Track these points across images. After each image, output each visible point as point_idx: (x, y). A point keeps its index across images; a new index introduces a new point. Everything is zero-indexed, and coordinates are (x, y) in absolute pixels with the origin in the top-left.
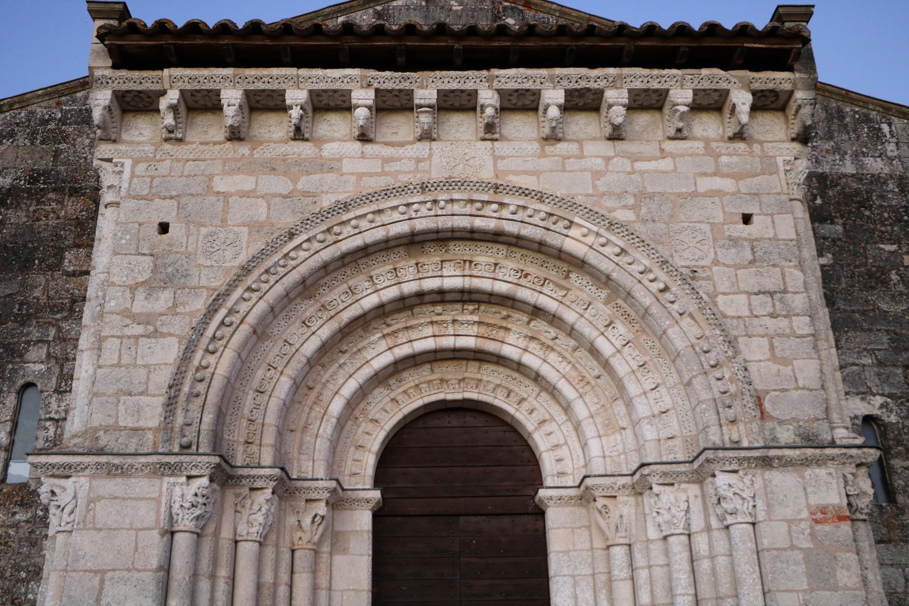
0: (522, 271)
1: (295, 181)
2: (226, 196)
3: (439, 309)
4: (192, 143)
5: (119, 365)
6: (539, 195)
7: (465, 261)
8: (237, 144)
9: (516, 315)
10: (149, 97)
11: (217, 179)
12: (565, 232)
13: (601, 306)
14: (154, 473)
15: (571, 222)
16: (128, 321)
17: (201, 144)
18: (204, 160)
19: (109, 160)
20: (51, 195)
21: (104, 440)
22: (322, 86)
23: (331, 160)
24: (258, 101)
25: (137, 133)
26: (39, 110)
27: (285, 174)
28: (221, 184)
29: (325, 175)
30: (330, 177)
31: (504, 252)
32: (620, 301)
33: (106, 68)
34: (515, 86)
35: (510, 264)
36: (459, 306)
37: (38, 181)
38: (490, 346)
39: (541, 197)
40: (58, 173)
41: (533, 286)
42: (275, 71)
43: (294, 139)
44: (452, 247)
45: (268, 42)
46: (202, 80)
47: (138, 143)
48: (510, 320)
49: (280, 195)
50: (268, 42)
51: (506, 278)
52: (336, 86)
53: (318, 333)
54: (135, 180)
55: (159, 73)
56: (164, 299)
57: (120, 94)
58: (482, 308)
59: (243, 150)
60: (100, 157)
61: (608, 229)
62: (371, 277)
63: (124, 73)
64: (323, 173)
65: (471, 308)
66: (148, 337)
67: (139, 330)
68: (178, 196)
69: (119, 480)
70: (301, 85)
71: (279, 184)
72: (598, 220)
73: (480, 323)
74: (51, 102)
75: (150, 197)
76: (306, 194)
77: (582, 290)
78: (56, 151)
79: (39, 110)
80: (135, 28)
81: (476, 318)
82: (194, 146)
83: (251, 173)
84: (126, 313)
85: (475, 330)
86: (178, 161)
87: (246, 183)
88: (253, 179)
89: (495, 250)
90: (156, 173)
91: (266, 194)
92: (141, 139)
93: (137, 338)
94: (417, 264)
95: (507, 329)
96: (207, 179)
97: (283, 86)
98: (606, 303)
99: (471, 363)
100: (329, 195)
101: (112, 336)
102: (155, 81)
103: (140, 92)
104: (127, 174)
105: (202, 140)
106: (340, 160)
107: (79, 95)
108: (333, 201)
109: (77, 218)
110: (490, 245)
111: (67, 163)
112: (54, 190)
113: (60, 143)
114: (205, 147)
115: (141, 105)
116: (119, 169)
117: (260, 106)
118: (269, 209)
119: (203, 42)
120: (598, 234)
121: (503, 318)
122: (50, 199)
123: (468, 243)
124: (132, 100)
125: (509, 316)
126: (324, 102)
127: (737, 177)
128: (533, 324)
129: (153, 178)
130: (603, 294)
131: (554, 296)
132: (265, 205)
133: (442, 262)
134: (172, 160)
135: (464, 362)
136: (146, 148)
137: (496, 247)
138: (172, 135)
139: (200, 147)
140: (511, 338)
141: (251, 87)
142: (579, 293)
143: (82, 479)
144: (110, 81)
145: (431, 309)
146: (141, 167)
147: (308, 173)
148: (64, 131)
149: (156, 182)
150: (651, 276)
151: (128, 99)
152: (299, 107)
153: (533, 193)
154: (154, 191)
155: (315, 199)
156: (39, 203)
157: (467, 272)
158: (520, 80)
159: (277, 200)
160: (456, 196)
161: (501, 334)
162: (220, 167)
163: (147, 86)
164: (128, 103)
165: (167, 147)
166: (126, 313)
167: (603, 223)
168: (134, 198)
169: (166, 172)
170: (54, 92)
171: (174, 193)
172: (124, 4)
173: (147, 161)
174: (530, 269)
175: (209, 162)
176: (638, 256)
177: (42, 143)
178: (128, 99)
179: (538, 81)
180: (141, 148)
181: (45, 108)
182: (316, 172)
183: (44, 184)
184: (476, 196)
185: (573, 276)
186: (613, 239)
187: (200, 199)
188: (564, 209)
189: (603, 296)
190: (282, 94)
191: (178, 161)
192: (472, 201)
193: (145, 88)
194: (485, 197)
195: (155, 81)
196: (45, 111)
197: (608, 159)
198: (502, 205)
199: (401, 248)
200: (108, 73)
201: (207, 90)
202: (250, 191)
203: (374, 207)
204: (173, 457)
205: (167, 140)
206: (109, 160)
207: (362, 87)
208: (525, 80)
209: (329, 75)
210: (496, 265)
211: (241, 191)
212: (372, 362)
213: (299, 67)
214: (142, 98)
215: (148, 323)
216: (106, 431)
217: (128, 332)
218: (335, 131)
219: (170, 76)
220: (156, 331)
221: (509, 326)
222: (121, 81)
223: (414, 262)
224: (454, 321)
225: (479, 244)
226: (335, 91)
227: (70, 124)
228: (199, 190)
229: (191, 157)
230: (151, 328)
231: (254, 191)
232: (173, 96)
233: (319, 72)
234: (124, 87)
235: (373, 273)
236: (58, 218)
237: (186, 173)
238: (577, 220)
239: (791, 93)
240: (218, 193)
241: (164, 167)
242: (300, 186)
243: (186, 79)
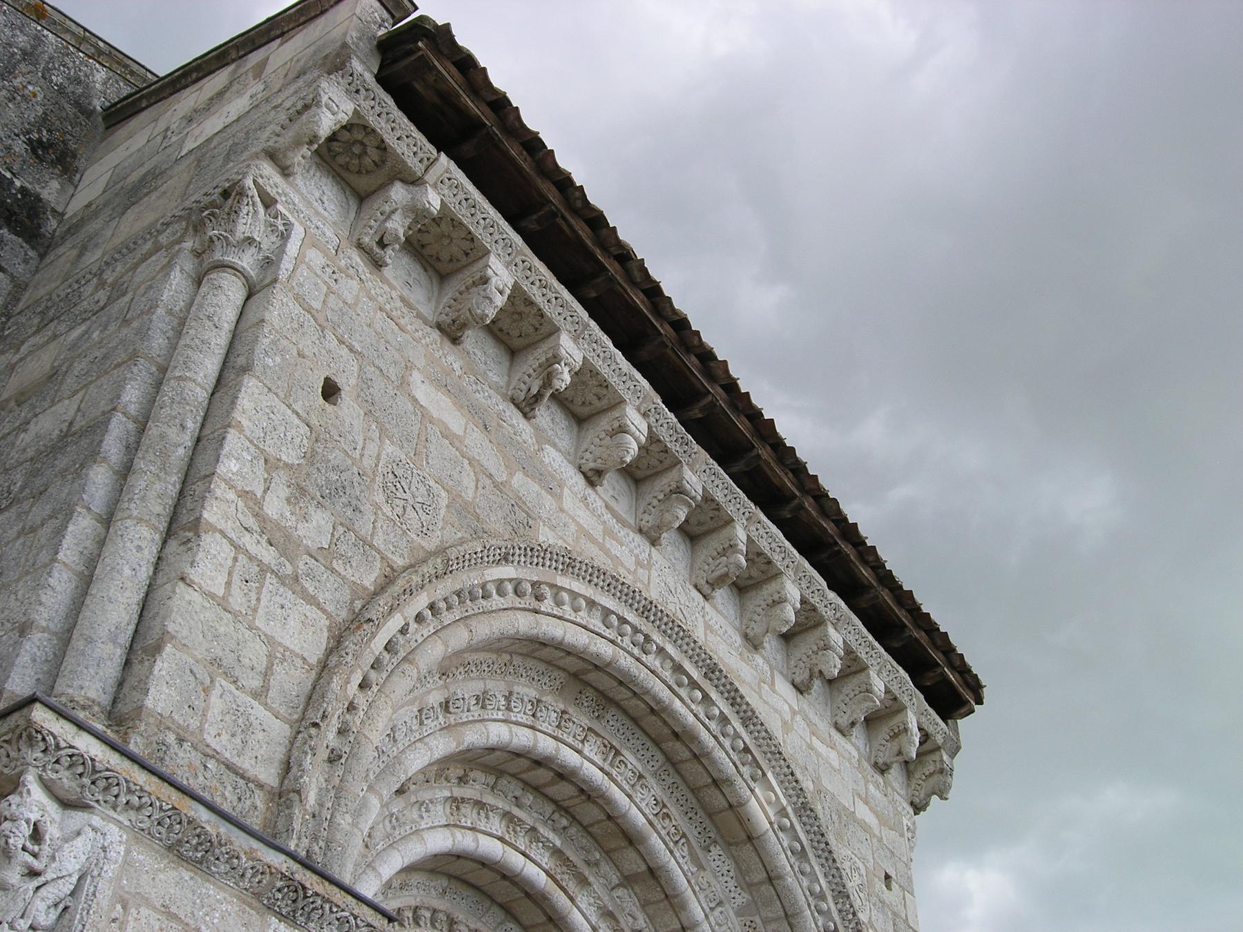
0: (664, 806)
3: (529, 799)
5: (223, 603)
6: (750, 714)
7: (612, 747)
9: (606, 867)
11: (415, 374)
12: (752, 784)
13: (731, 913)
14: (257, 896)
15: (764, 774)
16: (251, 522)
17: (403, 299)
21: (181, 762)
28: (423, 392)
31: (657, 765)
32: (757, 919)
34: (767, 551)
35: (657, 790)
36: (549, 808)
38: (560, 899)
39: (749, 718)
41: (667, 838)
44: (609, 716)
46: (479, 216)
48: (595, 869)
51: (643, 805)
52: (614, 380)
53: (427, 740)
56: (315, 528)
58: (573, 830)
61: (795, 810)
62: (511, 693)
65: (565, 822)
66: (282, 580)
67: (268, 555)
69: (187, 875)
72: (791, 792)
73: (557, 853)
77: (716, 877)
81: (558, 843)
84: (254, 503)
85: (546, 860)
89: (649, 754)
93: (264, 569)
94: (564, 712)
95: (583, 882)
98: (739, 913)
99: (495, 909)
101: (222, 532)
102: (421, 155)
110: (649, 744)
119: (531, 173)
120: (782, 812)
121: (588, 863)
123: (628, 723)
125: (597, 864)
127: (883, 821)
128: (620, 892)
130: (742, 898)
131: (686, 868)
133: (589, 729)
135: (487, 903)
137: (654, 750)
138: (377, 250)
140: (583, 900)
142: (713, 882)
143: (113, 829)
144: (363, 91)
145: (518, 793)
150: (824, 906)
153: (744, 707)
157: (607, 767)
158: (774, 545)
160: (670, 649)
161: (572, 886)
165: (357, 258)
166: (254, 503)
167: (795, 799)
171: (358, 347)
174: (673, 810)
176: (817, 868)
179: (787, 561)
184: (688, 666)
185: (716, 851)
186: (798, 827)
188: (765, 752)
189: (739, 900)
192: (678, 668)
193: (399, 151)
194: (695, 674)
195: (421, 155)
197: (794, 713)
198: (706, 696)
199: (563, 674)
203: (588, 591)
204: (315, 878)
207: (638, 410)
208: (778, 550)
210: (641, 777)
212: (426, 835)
215: (283, 554)
216: (181, 741)
217: (248, 541)
220: (296, 579)
221: (591, 879)
223: (562, 706)
224: (533, 829)
225: (639, 733)
228: (392, 372)
230: (289, 569)
234: (372, 120)
235: (516, 689)
238: (770, 775)
239: (938, 748)
243: (461, 196)
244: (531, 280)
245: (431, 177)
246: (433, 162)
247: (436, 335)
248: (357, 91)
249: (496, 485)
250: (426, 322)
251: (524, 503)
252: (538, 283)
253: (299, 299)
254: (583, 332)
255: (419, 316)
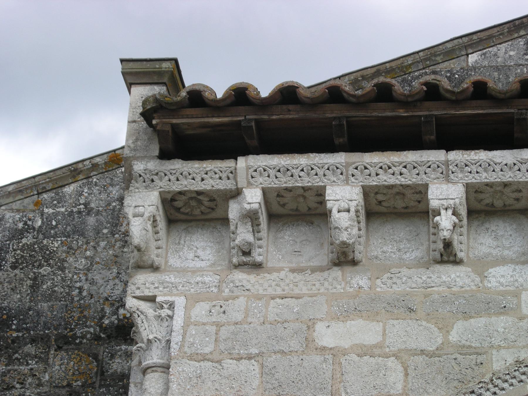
1: (445, 329)
2: (336, 353)
4: (279, 270)
8: (348, 269)
10: (212, 200)
11: (320, 327)
17: (293, 271)
18: (297, 298)
19: (151, 299)
20: (30, 349)
22: (485, 177)
23: (504, 294)
24: (380, 202)
25: (191, 255)
26: (8, 215)
27: (428, 317)
28: (327, 335)
29: (494, 319)
30: (501, 323)
33: (151, 158)
37: (9, 327)
40: (39, 314)
42: (411, 156)
43: (442, 262)
45: (402, 113)
46: (296, 172)
47: (195, 271)
49: (423, 352)
50: (402, 113)
52: (508, 176)
54: (192, 330)
55: (229, 164)
57: (169, 197)
59: (359, 280)
60: (138, 293)
63: (177, 165)
64: (489, 315)
68: (260, 354)
70: (452, 176)
71: (420, 335)
74: (26, 201)
75: (216, 357)
76: (464, 350)
78: (35, 279)
79: (8, 215)
80: (197, 98)
82: (282, 274)
83: (373, 316)
86: (259, 298)
87: (365, 332)
88: (378, 327)
90: (223, 319)
91: (400, 351)
92: (199, 264)
96: (305, 327)
97: (423, 179)
100: (503, 352)
102: (224, 176)
103: (199, 193)
104: (178, 322)
105: (294, 265)
106: (517, 295)
107: (69, 190)
108: (511, 360)
109: (69, 385)
111: (51, 296)
112: (33, 341)
113: (40, 266)
114: (298, 277)
115: (197, 212)
116: (165, 312)
117: (382, 209)
118: (407, 375)
119: (301, 115)
122: (28, 355)
124: (186, 204)
126: (487, 201)
129: (219, 325)
132: (400, 368)
134: (248, 297)
136: (207, 279)
139: (291, 276)
141: (373, 182)
144: (155, 178)
146: (200, 311)
147: (466, 316)
148: (47, 247)
149: (224, 332)
151: (177, 204)
152: (450, 212)
154: (222, 346)
155: (480, 359)
156: (10, 361)
159: (420, 359)
162: (325, 308)
163: (211, 184)
164: (178, 209)
165: (240, 276)
168: (191, 358)
169: (239, 317)
170: (31, 188)
171: (254, 351)
172: (176, 61)
173: (210, 299)
175: (306, 299)
177: (14, 267)
178: (177, 204)
180: (199, 279)
181: (18, 211)
182: (478, 314)
183: (17, 330)
187: (295, 360)
190: (421, 191)
191: (259, 298)
193: (209, 188)
195: (224, 176)
196: (18, 216)
200: (153, 165)
201: (303, 188)
202: (375, 346)
205: (239, 266)
206: (151, 299)
209: (498, 160)
211: (361, 346)
213: (448, 149)
214: (200, 202)
218: (504, 248)
219: (248, 168)
222: (173, 178)
226: (506, 185)
227: (55, 236)
228: (295, 344)
229: (279, 291)
231: (379, 346)
232: (253, 197)
233: (482, 155)
234: (176, 187)
236: (40, 385)
237: (271, 317)
240: (324, 349)
241: (236, 310)
242: (454, 337)
243: (272, 172)
244: (373, 174)
245: (242, 182)
246: (234, 172)
247: (337, 272)
248: (153, 181)
249: (431, 355)
250: (322, 269)
251: (470, 347)
252: (381, 171)
253: (193, 357)
254: (448, 169)
255: (314, 270)
